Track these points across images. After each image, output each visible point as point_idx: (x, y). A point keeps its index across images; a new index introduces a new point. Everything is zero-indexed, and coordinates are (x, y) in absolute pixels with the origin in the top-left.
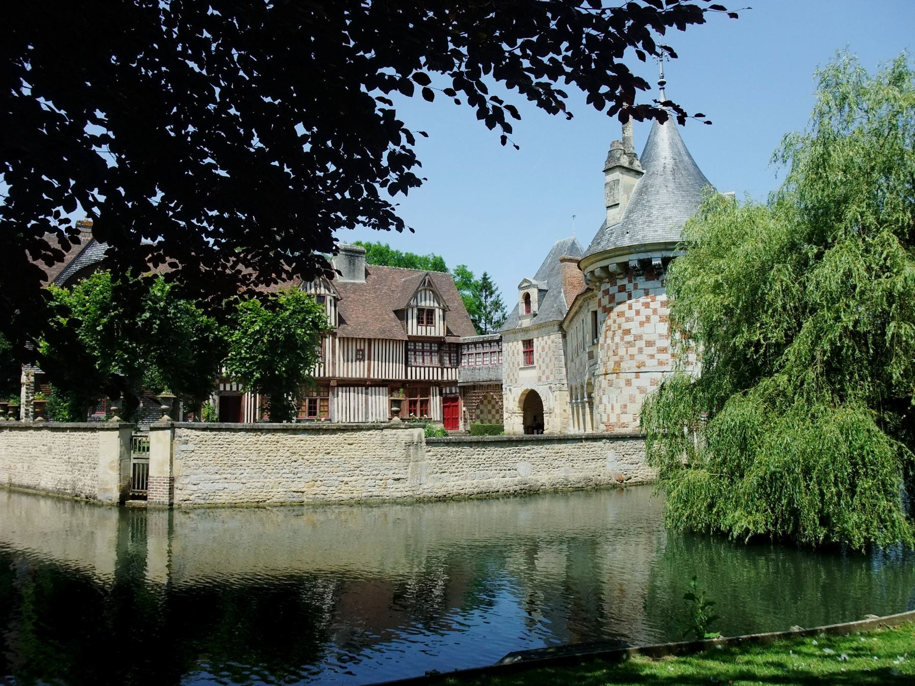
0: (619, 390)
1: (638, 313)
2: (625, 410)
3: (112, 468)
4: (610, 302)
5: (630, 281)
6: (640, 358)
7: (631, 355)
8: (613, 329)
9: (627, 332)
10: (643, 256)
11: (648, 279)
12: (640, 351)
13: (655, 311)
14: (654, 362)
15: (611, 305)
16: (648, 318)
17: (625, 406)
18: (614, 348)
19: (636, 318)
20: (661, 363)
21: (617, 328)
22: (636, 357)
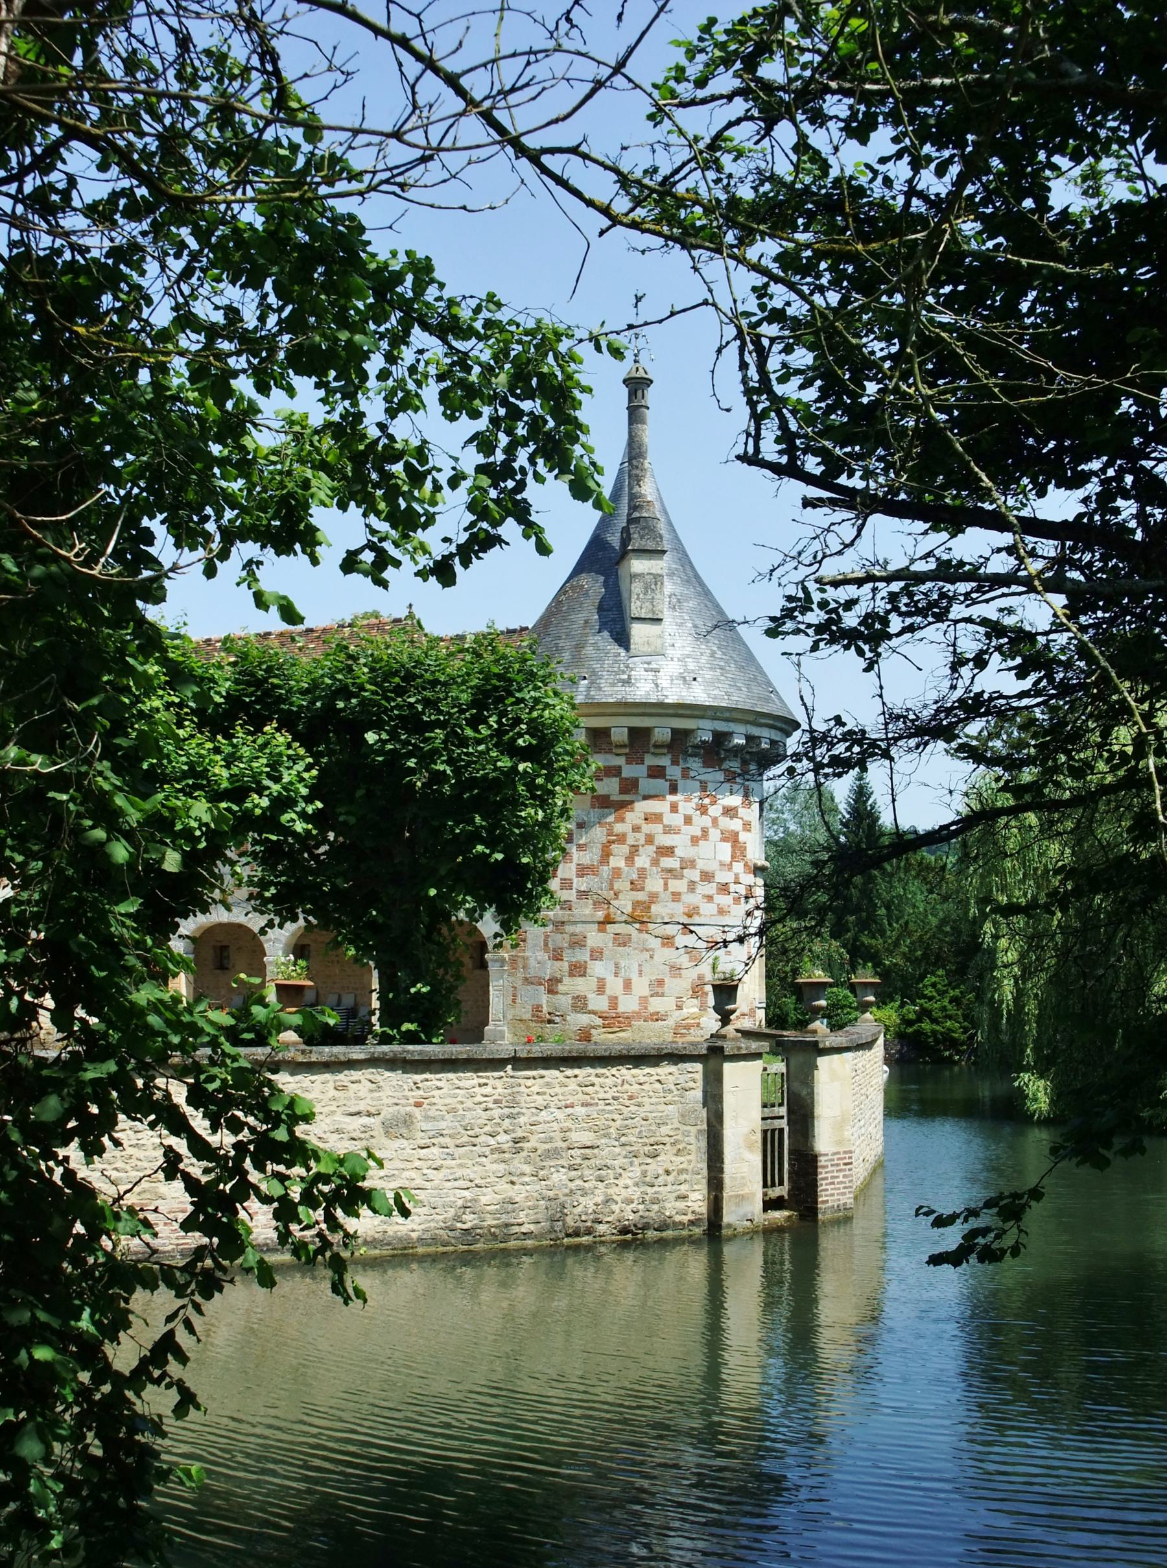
0: (647, 955)
1: (688, 820)
2: (660, 990)
3: (750, 1147)
4: (623, 791)
5: (675, 762)
6: (690, 899)
7: (673, 894)
8: (630, 840)
9: (669, 851)
10: (721, 726)
11: (706, 764)
12: (692, 886)
13: (715, 821)
14: (711, 909)
15: (626, 797)
16: (705, 832)
17: (661, 983)
18: (635, 876)
19: (685, 829)
20: (722, 912)
21: (642, 841)
22: (683, 897)
